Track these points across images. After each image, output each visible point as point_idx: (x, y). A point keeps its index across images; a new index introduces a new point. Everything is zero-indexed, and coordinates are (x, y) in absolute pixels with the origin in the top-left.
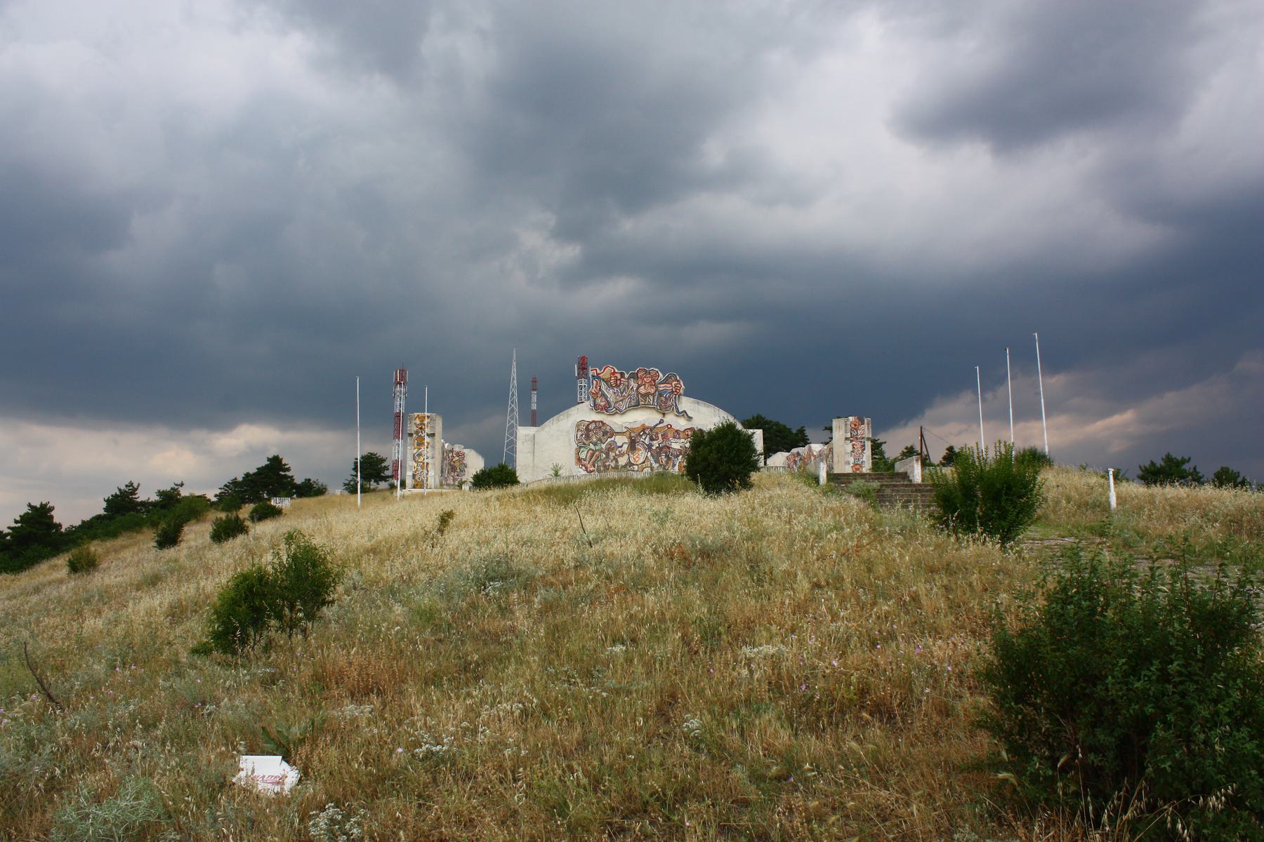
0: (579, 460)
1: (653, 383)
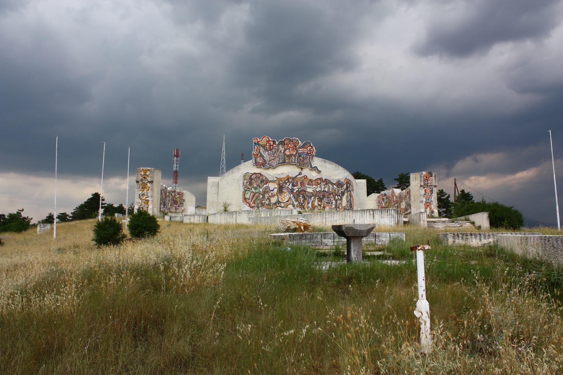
0: (245, 199)
1: (295, 148)
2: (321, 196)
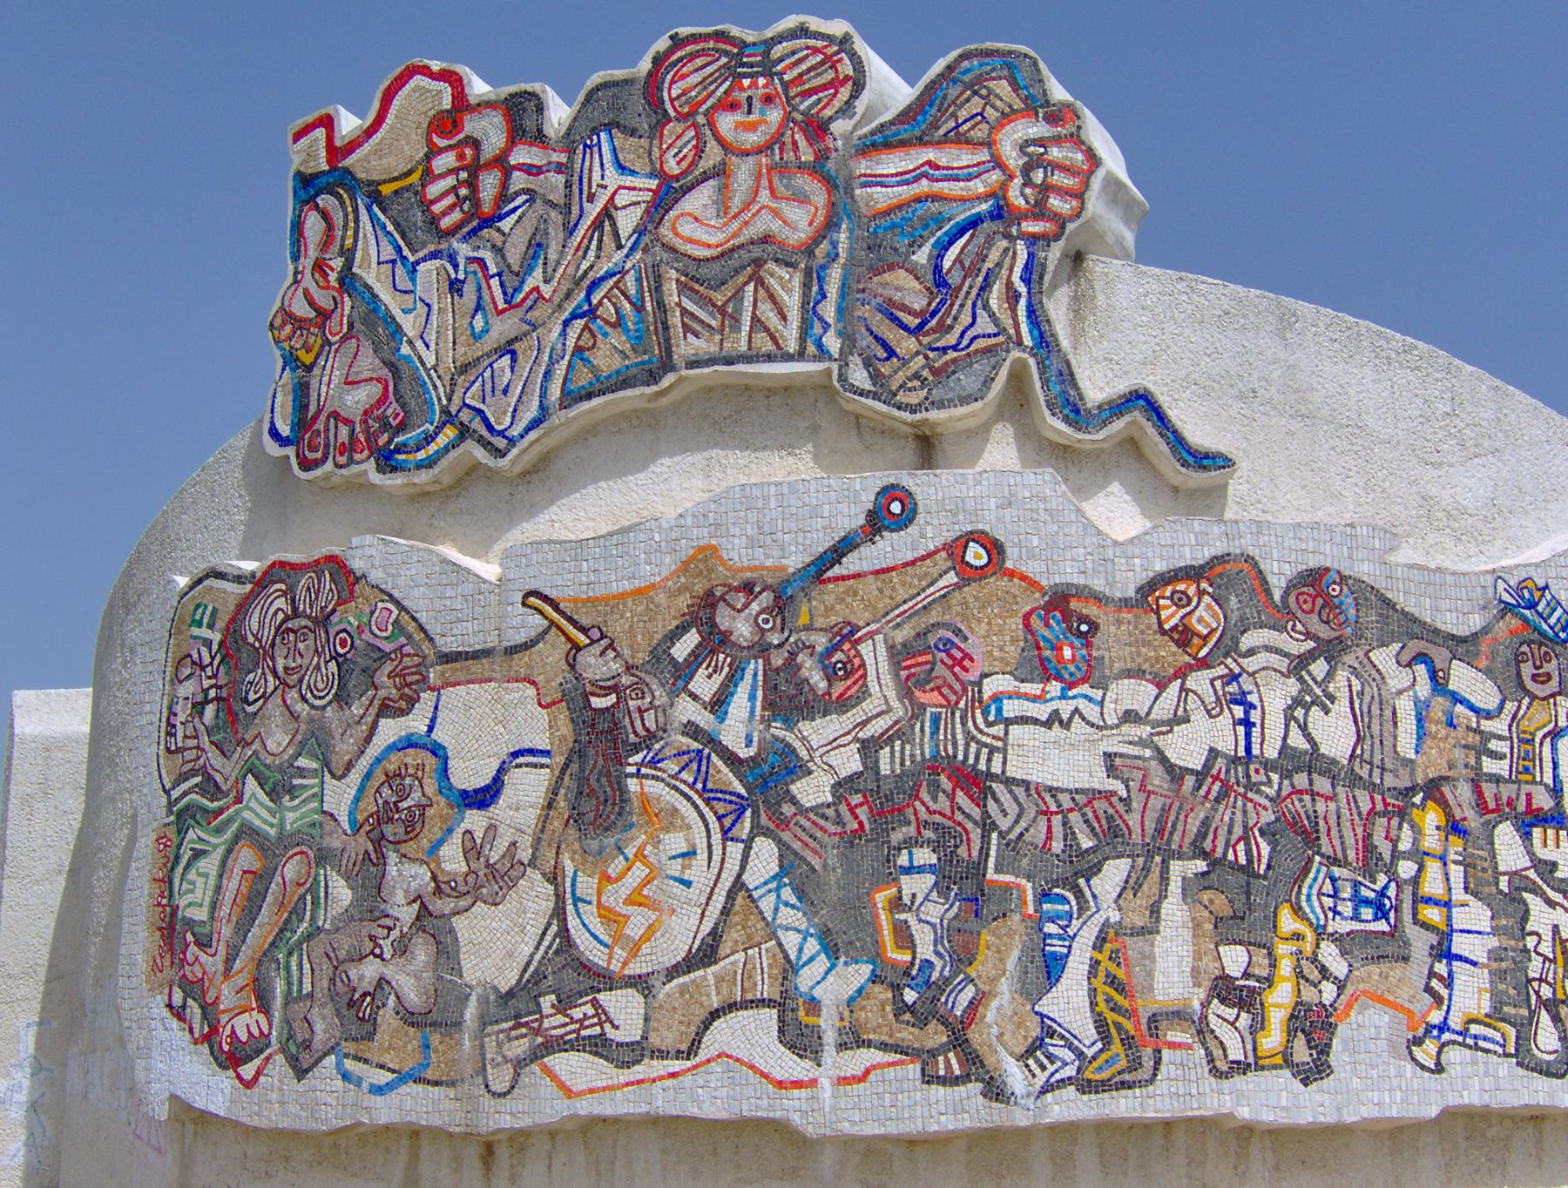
2: (1260, 847)
